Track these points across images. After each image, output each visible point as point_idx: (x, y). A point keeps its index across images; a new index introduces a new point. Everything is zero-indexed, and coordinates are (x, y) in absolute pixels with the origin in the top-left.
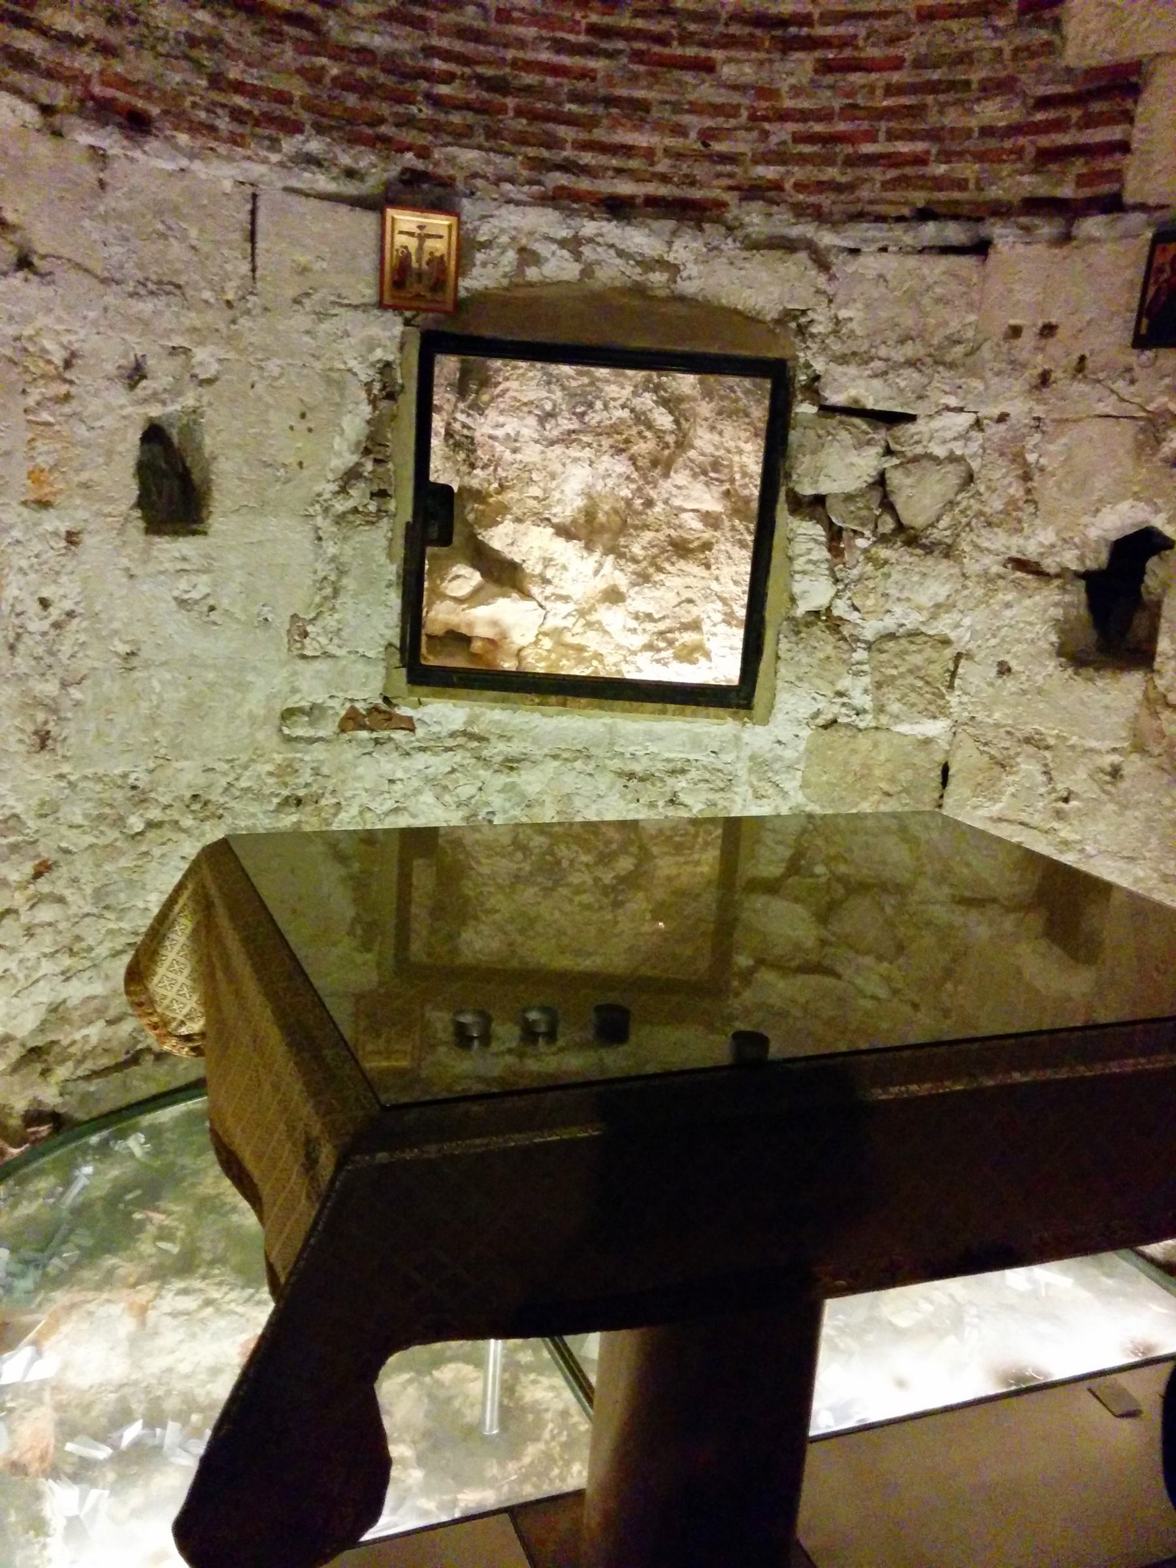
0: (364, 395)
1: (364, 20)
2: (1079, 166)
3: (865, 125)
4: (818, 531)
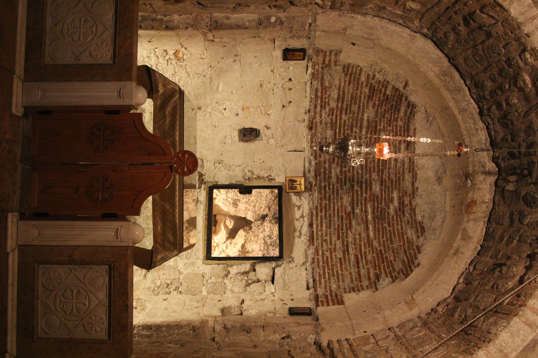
2: (324, 300)
3: (330, 268)
4: (247, 269)
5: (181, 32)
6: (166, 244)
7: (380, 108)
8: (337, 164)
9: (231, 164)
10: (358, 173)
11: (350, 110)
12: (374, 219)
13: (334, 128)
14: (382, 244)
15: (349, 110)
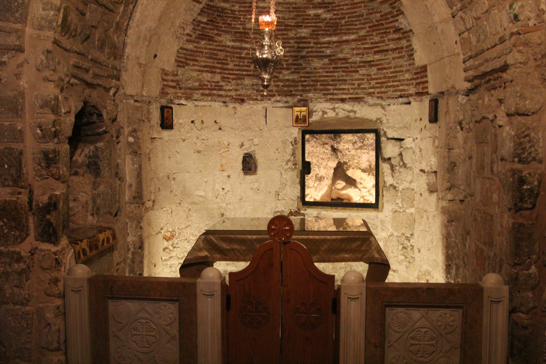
0: (290, 144)
1: (287, 74)
2: (421, 86)
3: (388, 80)
5: (145, 234)
6: (363, 248)
7: (221, 29)
8: (280, 73)
9: (279, 183)
10: (288, 52)
11: (223, 60)
12: (336, 35)
13: (242, 77)
14: (363, 26)
15: (224, 61)
